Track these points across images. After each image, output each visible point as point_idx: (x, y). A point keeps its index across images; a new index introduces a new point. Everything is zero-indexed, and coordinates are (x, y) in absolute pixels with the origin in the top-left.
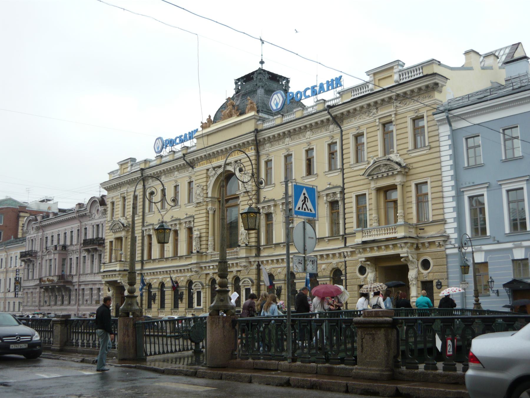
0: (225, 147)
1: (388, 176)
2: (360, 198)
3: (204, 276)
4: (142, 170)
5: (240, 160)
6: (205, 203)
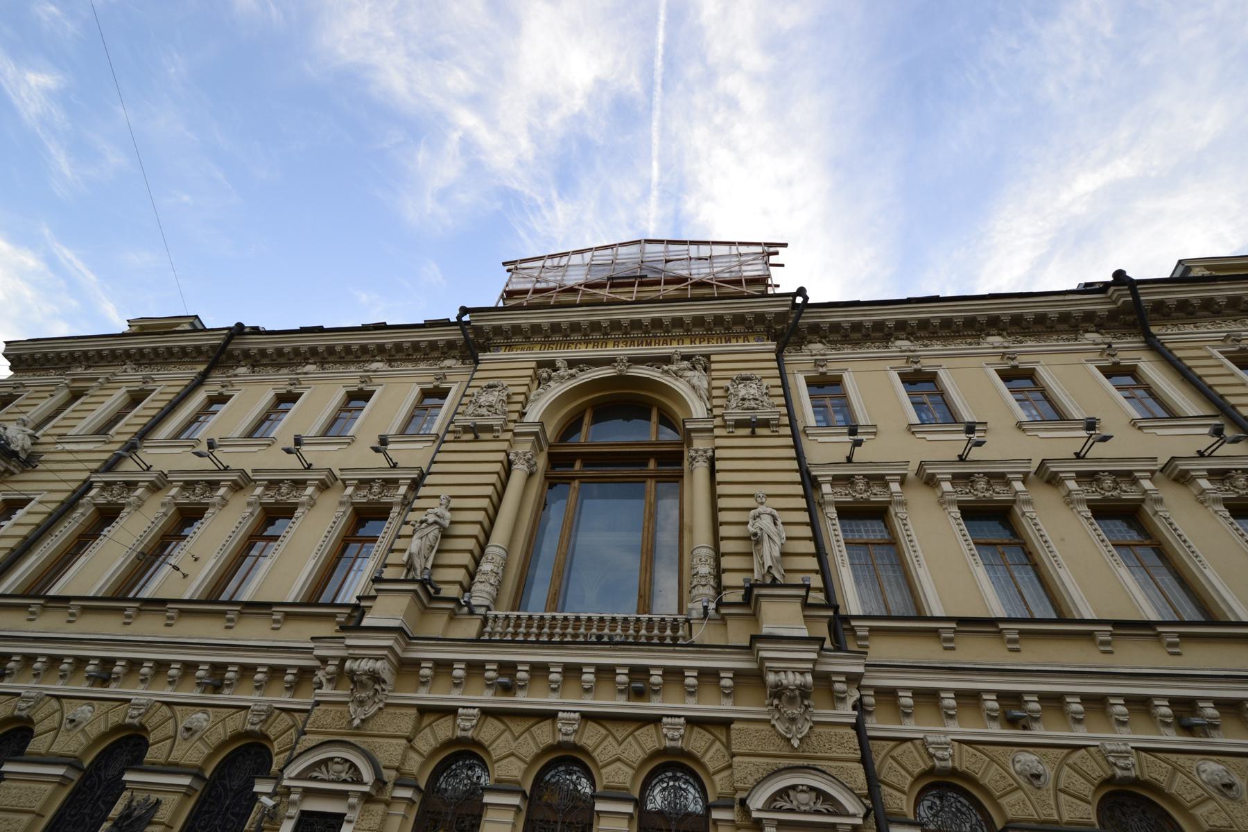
3: (405, 722)
5: (707, 356)
6: (509, 435)
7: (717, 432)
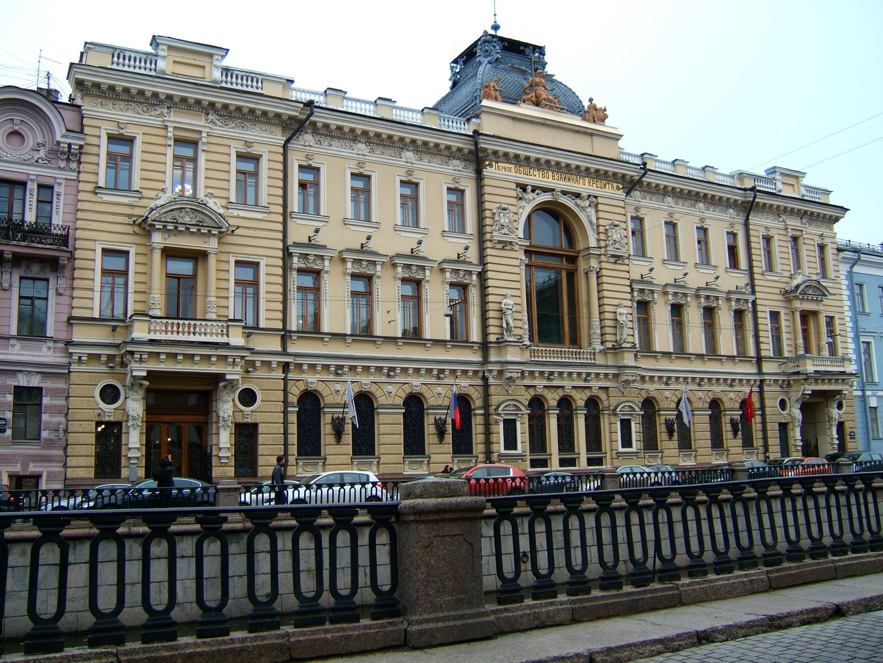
0: (579, 163)
1: (812, 300)
2: (775, 316)
4: (310, 104)
5: (596, 197)
7: (603, 258)
